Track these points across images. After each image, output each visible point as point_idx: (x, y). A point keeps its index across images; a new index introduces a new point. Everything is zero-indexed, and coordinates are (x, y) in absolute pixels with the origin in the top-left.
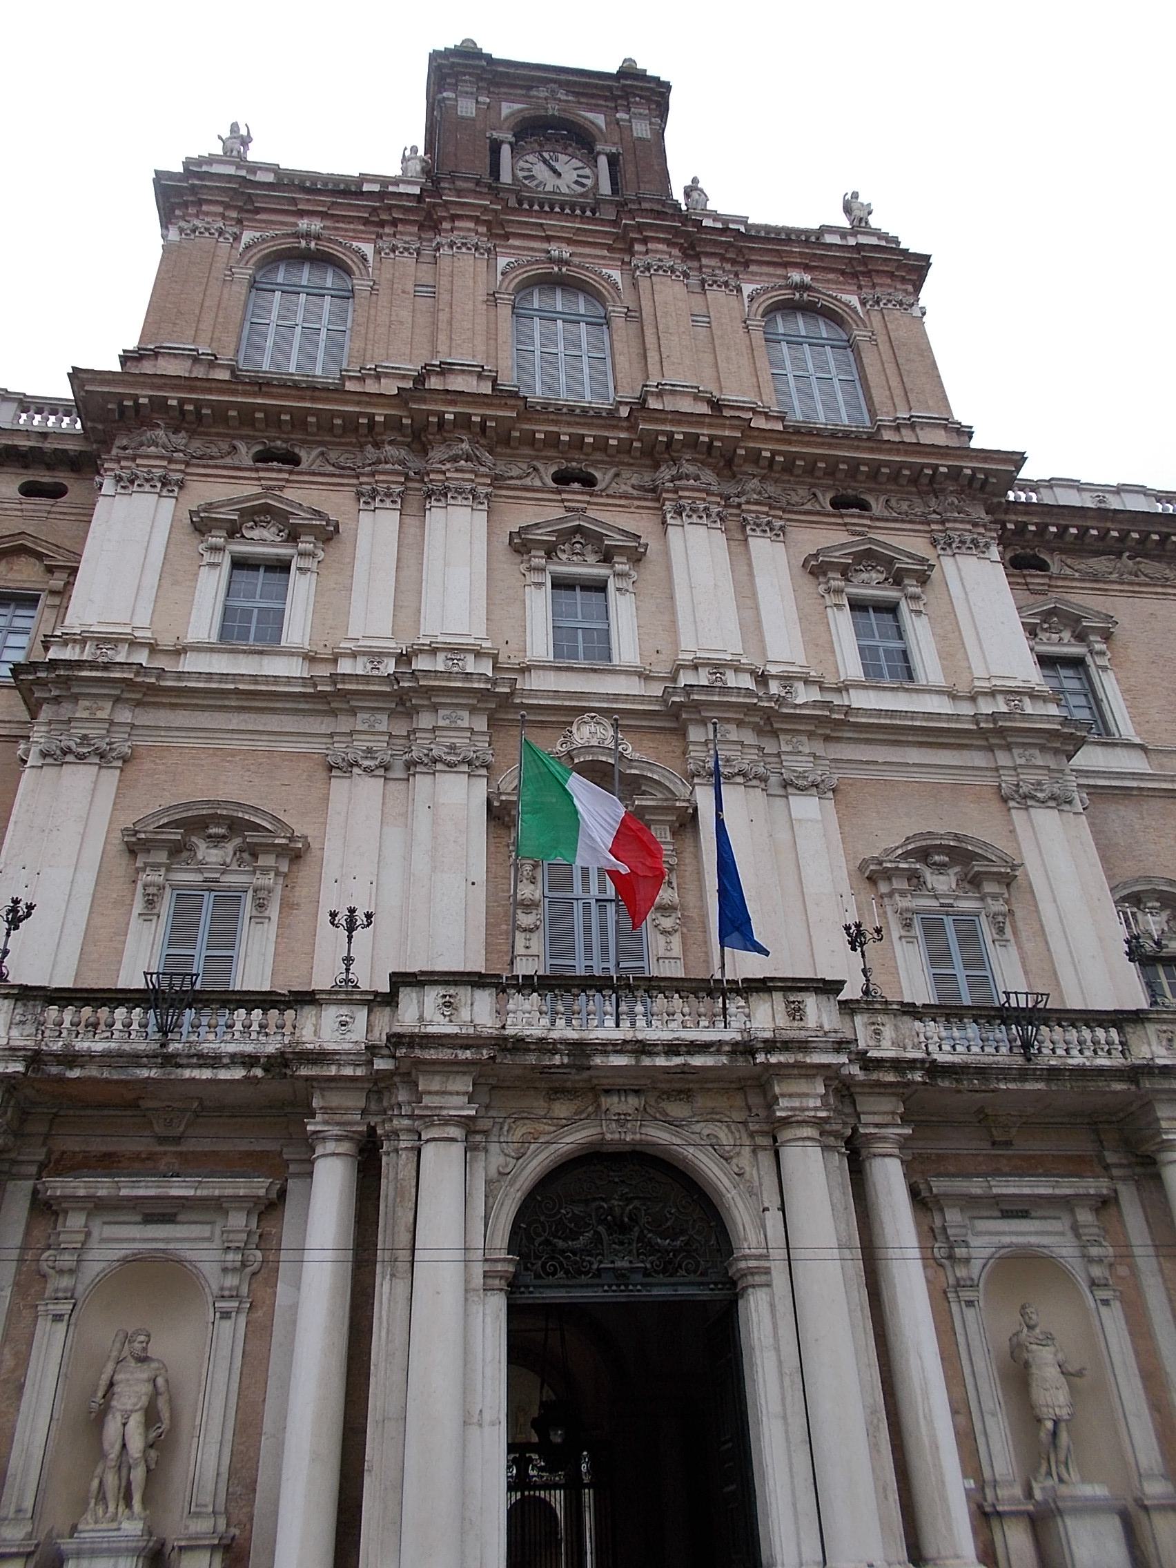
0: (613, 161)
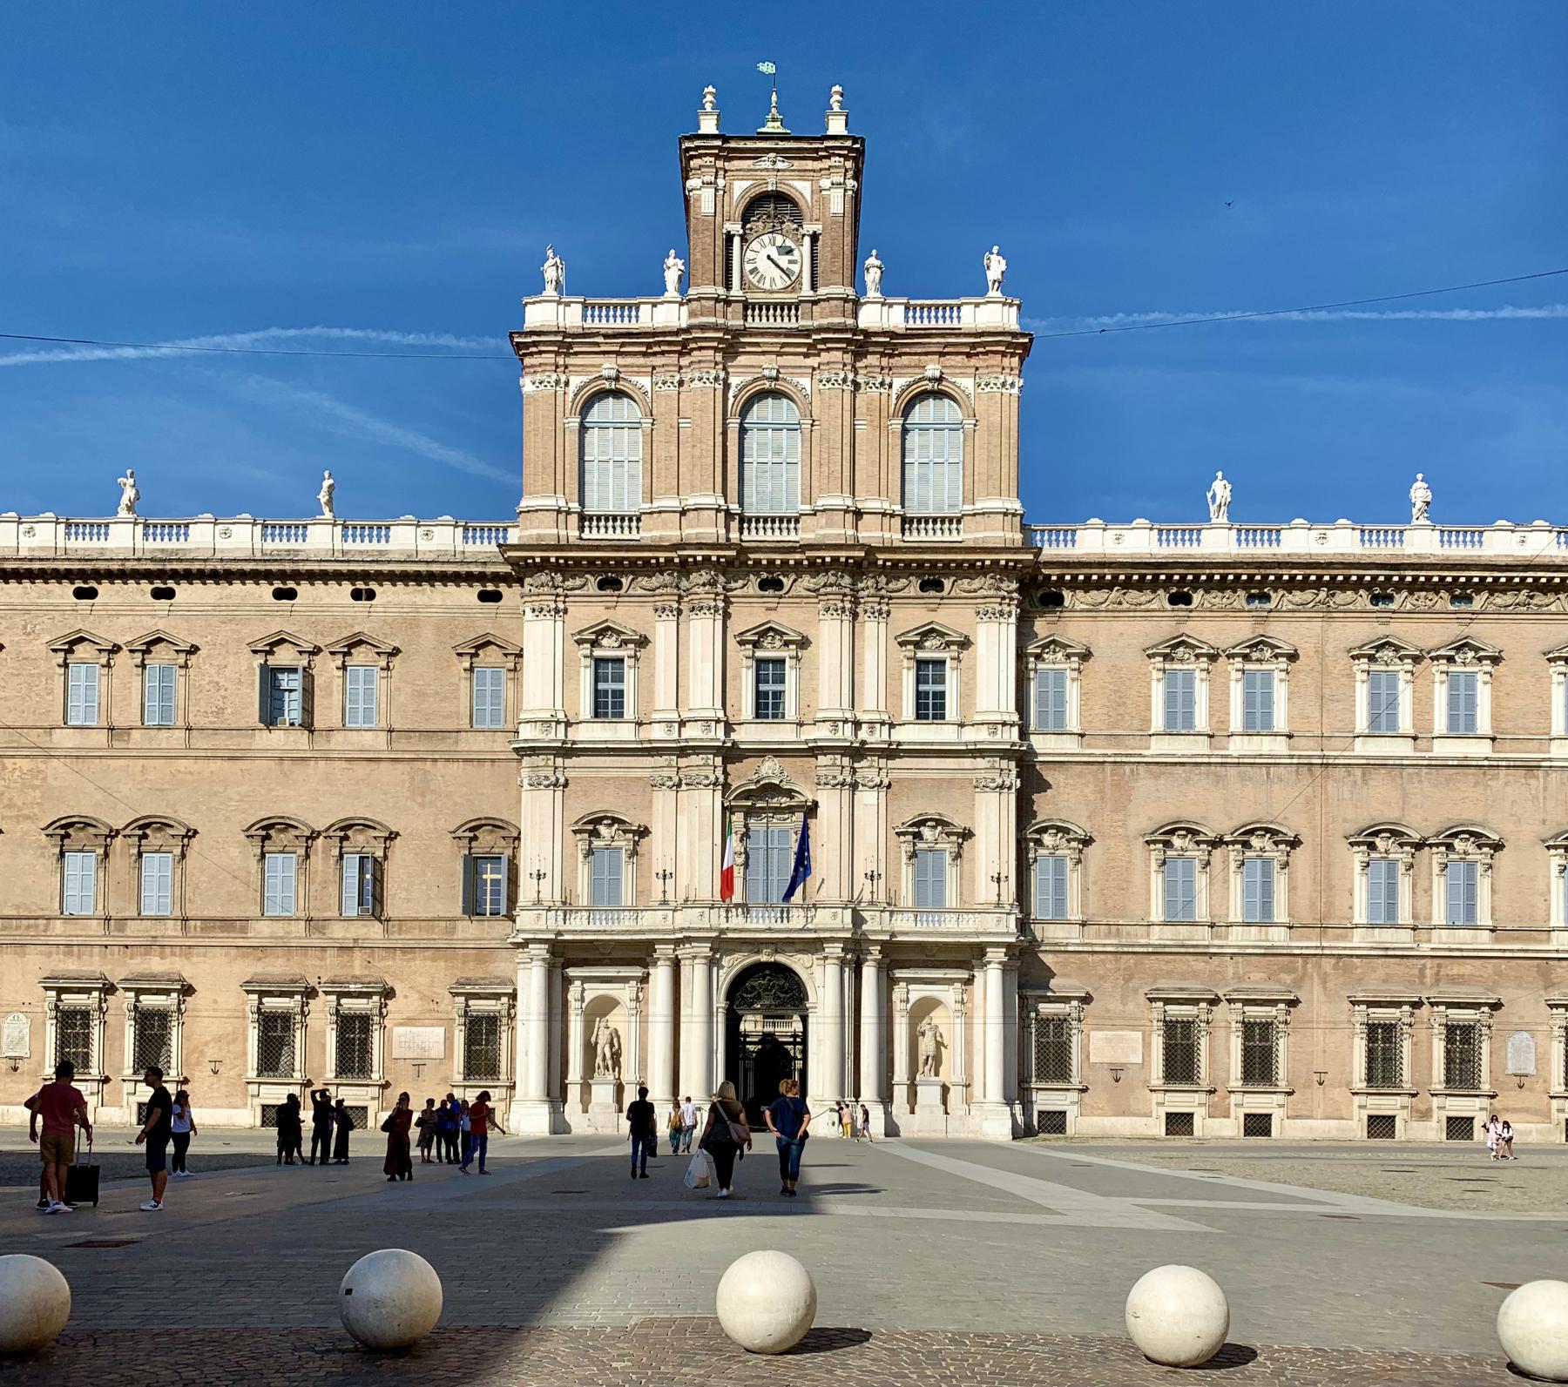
0: (815, 238)
